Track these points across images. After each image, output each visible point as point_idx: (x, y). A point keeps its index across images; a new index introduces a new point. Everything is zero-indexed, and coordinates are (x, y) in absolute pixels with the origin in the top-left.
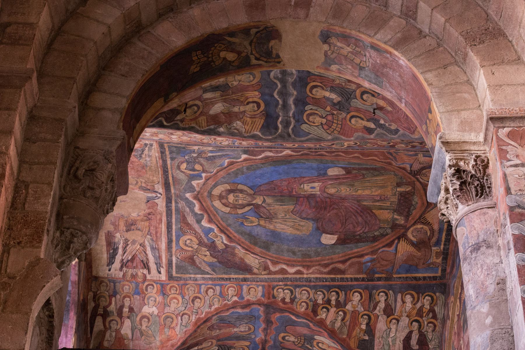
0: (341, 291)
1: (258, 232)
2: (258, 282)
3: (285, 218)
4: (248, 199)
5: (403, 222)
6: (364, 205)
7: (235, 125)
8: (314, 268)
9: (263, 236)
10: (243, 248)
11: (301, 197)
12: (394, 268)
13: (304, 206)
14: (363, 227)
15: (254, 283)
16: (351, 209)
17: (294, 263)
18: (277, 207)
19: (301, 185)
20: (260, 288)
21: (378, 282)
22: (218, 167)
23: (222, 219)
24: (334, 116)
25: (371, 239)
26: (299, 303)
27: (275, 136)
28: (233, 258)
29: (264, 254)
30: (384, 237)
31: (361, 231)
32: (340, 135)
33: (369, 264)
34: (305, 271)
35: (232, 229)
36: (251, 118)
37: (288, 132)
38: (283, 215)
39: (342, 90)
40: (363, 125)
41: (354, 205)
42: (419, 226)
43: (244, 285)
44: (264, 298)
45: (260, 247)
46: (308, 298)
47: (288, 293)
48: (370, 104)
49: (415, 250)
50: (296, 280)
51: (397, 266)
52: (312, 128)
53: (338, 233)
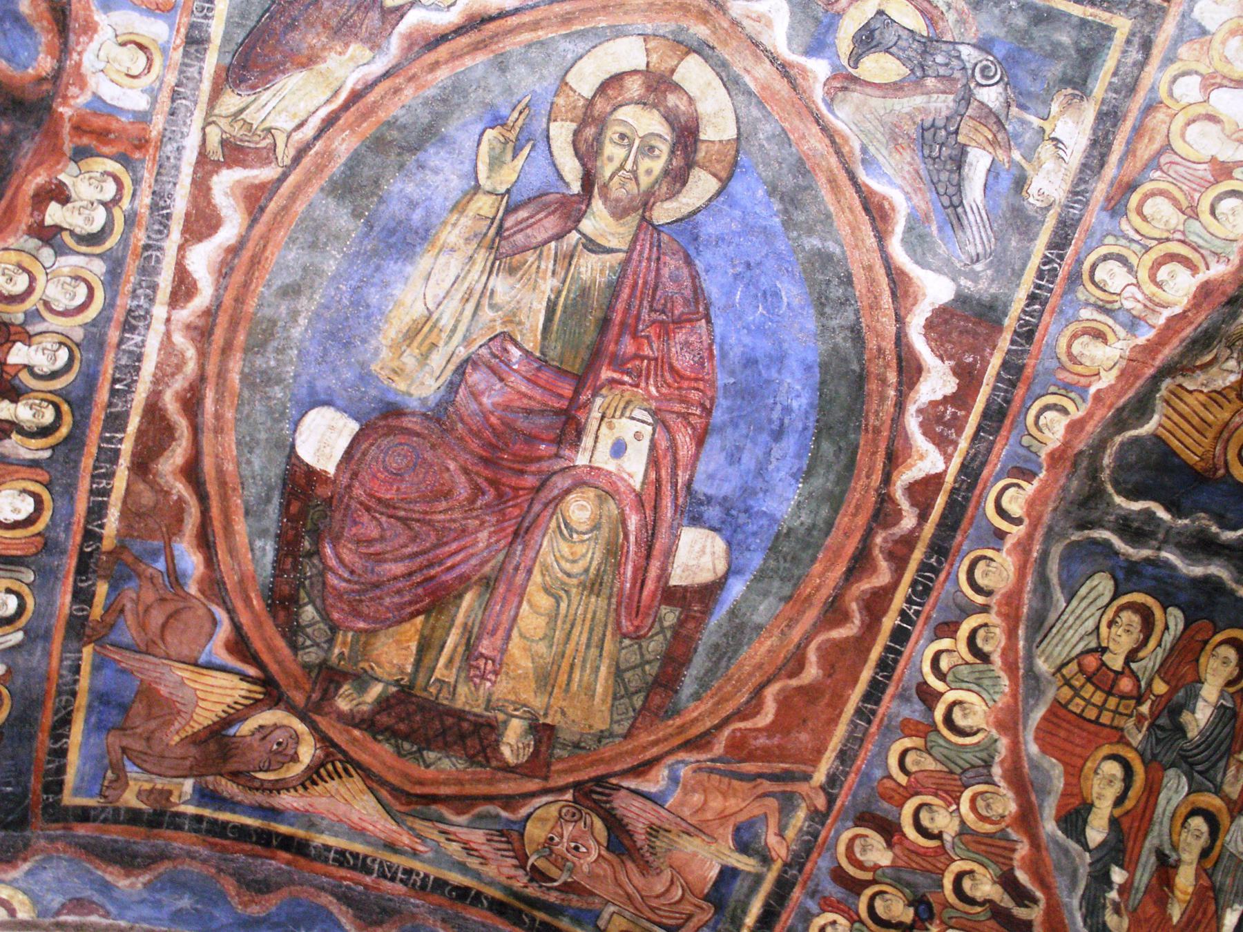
0: (53, 448)
1: (436, 171)
2: (175, 95)
3: (485, 301)
4: (623, 186)
5: (343, 705)
6: (460, 596)
7: (1232, 364)
8: (191, 353)
9: (410, 188)
10: (370, 86)
11: (577, 392)
12: (128, 653)
13: (523, 389)
14: (352, 572)
15: (171, 79)
16: (454, 546)
17: (238, 277)
18: (548, 285)
19: (654, 413)
20: (140, 102)
21: (70, 589)
22: (864, 150)
23: (542, 43)
24: (1133, 702)
25: (286, 589)
26: (27, 261)
27: (1105, 475)
28: (325, 25)
29: (320, 168)
30: (284, 636)
31: (333, 562)
32: (1052, 706)
33: (161, 565)
34: (186, 314)
35: (479, 72)
36: (1227, 424)
37: (1102, 527)
38: (498, 299)
39: (1223, 748)
40: (1097, 803)
41: (473, 562)
42: (307, 752)
43: (171, 27)
44: (88, 105)
45: (355, 161)
46: (46, 304)
47: (90, 220)
48: (1175, 838)
49: (197, 727)
50: (148, 270)
51: (130, 661)
52: (1093, 609)
53: (344, 480)
